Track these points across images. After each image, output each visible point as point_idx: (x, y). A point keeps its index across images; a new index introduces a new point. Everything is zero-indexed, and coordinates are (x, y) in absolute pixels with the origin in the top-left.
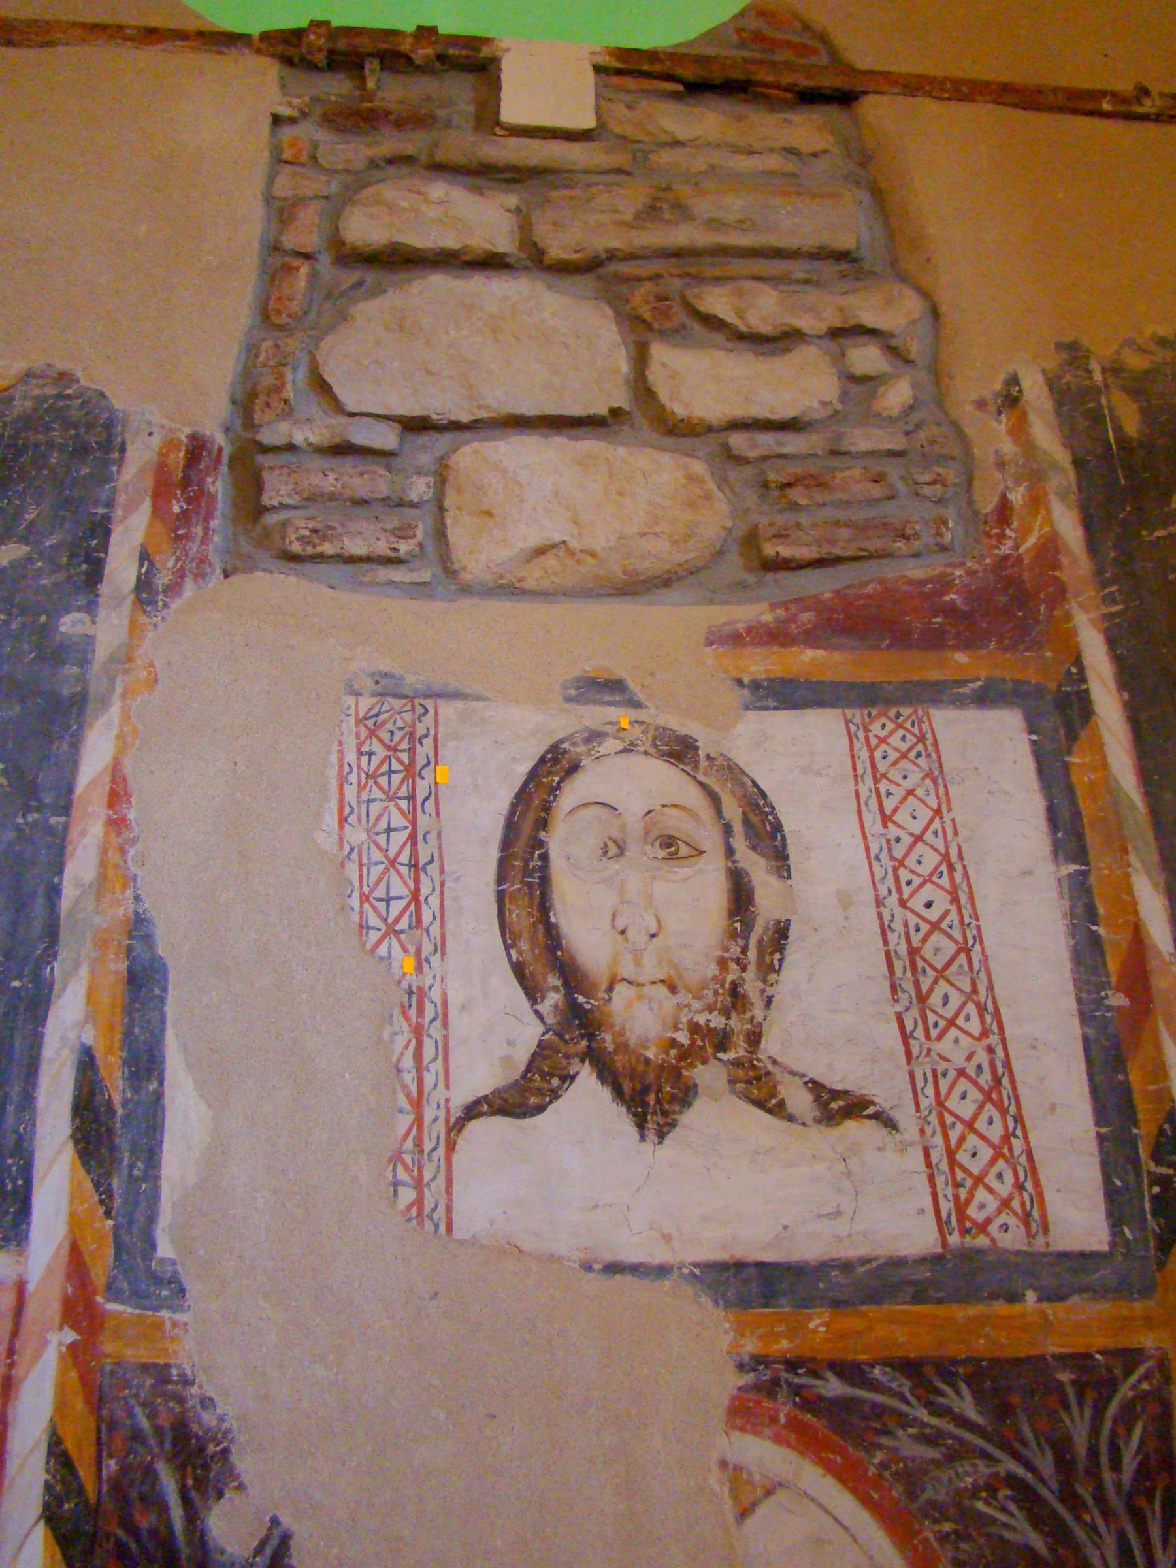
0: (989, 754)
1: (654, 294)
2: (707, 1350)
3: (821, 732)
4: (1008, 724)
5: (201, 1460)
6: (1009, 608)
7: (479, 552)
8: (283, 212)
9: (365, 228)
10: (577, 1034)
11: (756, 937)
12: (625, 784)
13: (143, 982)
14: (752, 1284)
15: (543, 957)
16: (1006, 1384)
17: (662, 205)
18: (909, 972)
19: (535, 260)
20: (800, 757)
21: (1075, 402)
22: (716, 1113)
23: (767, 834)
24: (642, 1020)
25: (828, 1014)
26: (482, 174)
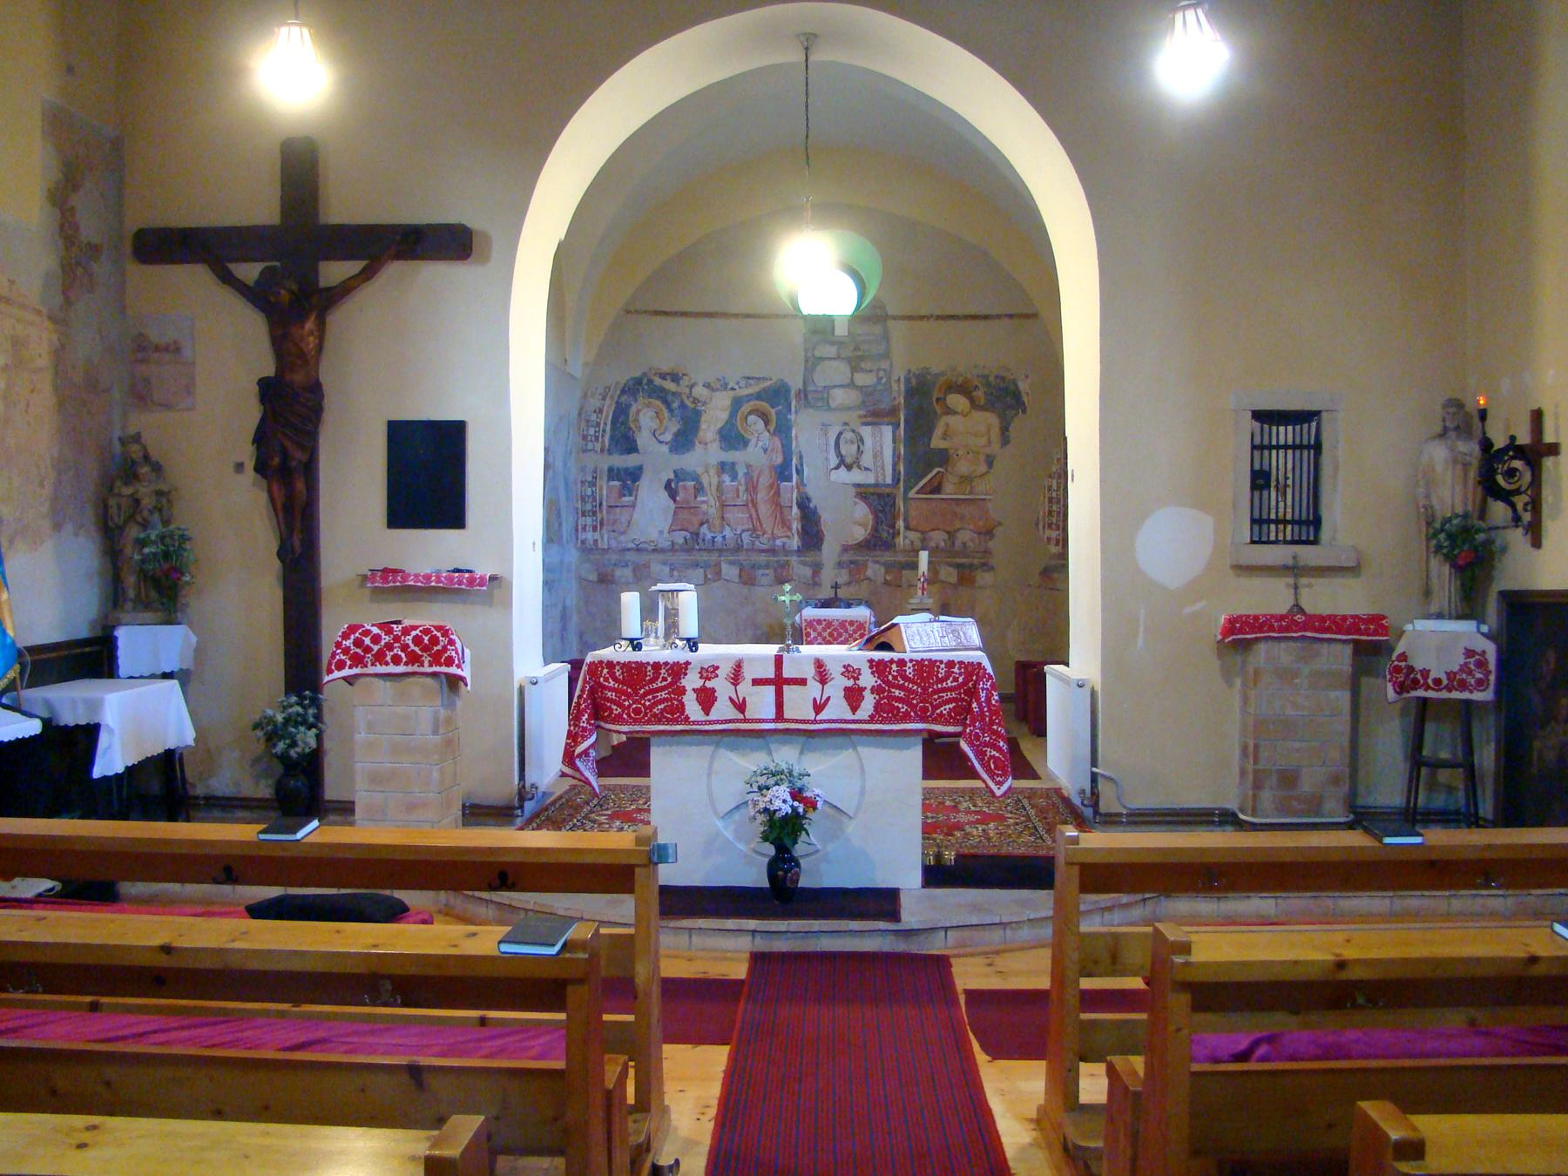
0: (887, 431)
1: (855, 365)
2: (853, 491)
3: (869, 428)
4: (890, 428)
5: (809, 500)
6: (893, 412)
7: (833, 405)
8: (806, 350)
9: (817, 354)
10: (842, 462)
11: (860, 452)
12: (848, 435)
13: (801, 458)
14: (858, 485)
15: (839, 454)
16: (880, 496)
17: (857, 348)
18: (875, 457)
19: (838, 358)
20: (866, 432)
21: (908, 380)
22: (855, 470)
23: (862, 440)
24: (849, 460)
25: (867, 460)
26: (832, 343)
